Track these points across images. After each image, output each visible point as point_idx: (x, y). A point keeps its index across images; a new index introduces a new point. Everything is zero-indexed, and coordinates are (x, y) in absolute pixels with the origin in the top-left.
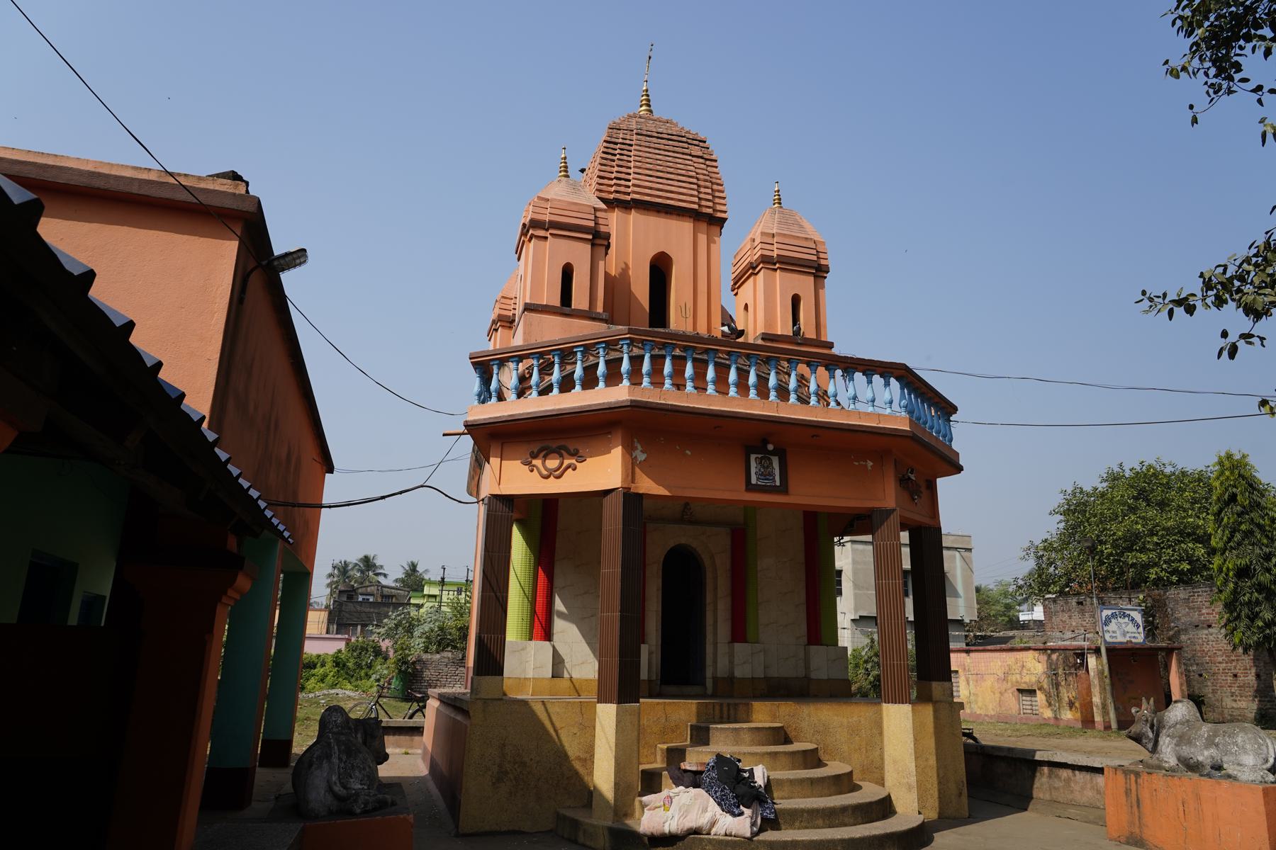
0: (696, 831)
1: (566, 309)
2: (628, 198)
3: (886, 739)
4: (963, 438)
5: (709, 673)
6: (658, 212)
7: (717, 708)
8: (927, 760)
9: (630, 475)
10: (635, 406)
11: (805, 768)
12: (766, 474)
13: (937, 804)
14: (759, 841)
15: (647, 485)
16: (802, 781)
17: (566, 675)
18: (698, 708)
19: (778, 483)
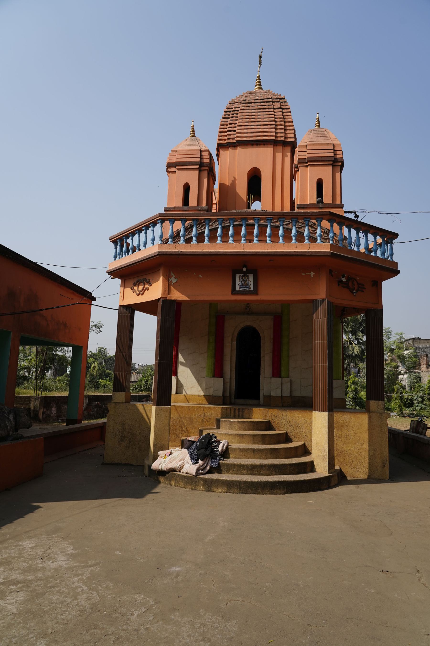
0: (174, 470)
1: (186, 208)
2: (234, 141)
3: (313, 431)
4: (400, 253)
5: (261, 394)
6: (252, 145)
7: (232, 411)
8: (362, 445)
9: (167, 289)
10: (160, 255)
11: (262, 444)
12: (245, 284)
13: (367, 470)
14: (199, 477)
15: (177, 295)
16: (247, 450)
17: (184, 393)
18: (222, 411)
19: (252, 289)
